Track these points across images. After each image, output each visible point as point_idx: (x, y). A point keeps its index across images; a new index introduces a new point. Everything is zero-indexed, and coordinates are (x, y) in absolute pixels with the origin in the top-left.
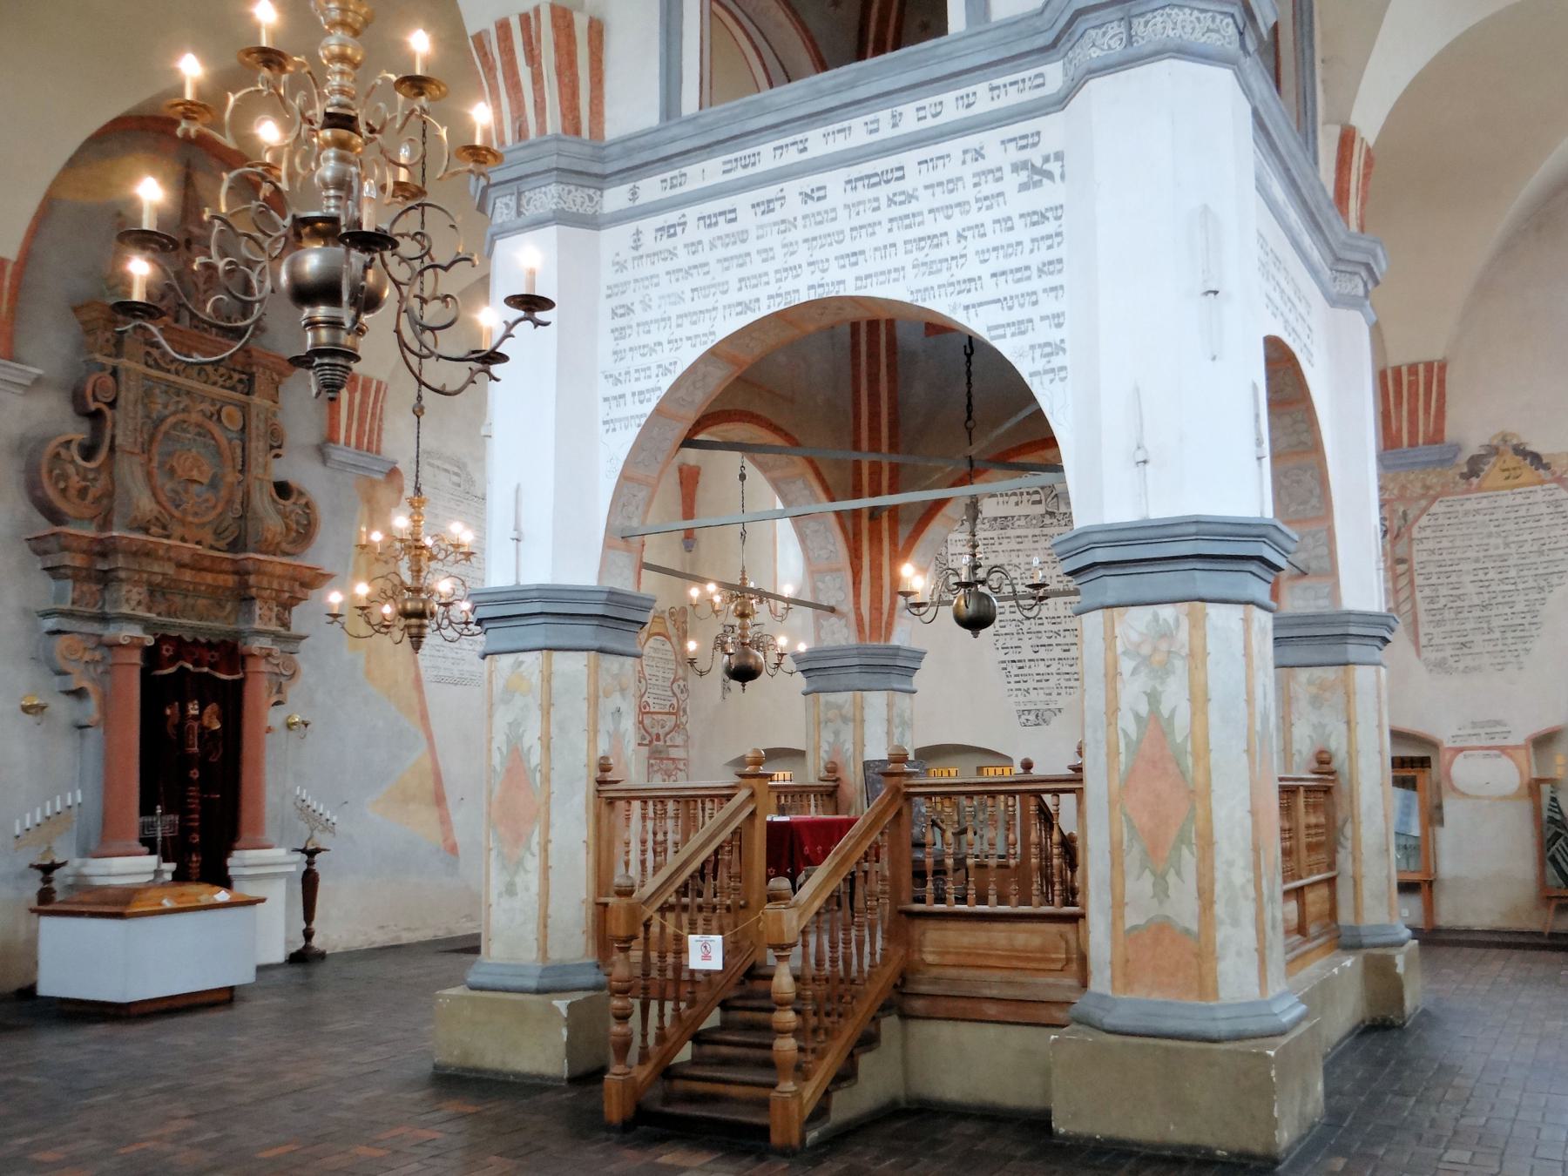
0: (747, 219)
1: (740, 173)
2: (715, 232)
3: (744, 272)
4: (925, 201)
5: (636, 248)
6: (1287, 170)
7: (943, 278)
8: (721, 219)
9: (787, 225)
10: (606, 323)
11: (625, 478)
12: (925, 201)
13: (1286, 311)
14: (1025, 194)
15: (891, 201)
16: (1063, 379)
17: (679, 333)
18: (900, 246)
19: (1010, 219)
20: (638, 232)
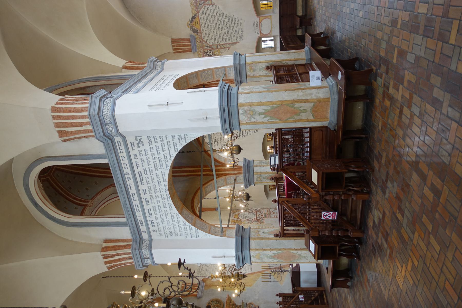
0: (150, 206)
1: (140, 208)
2: (153, 214)
3: (162, 207)
5: (157, 231)
6: (135, 83)
7: (164, 162)
8: (150, 212)
9: (151, 197)
10: (174, 238)
11: (209, 233)
12: (146, 167)
15: (146, 174)
17: (176, 221)
18: (156, 172)
20: (153, 231)
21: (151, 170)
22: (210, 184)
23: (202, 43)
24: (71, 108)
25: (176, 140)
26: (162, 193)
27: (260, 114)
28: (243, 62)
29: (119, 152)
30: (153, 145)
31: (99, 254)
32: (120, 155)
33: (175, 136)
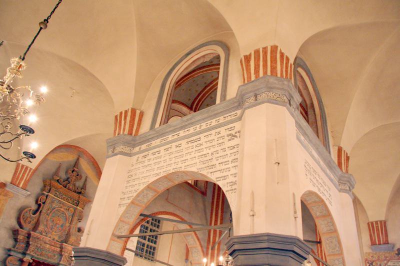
0: (163, 153)
2: (155, 156)
4: (205, 145)
7: (206, 165)
16: (235, 192)
19: (225, 148)
23: (385, 260)
24: (276, 63)
25: (231, 179)
26: (173, 164)
29: (225, 116)
30: (228, 152)
31: (129, 107)
32: (222, 118)
33: (235, 177)
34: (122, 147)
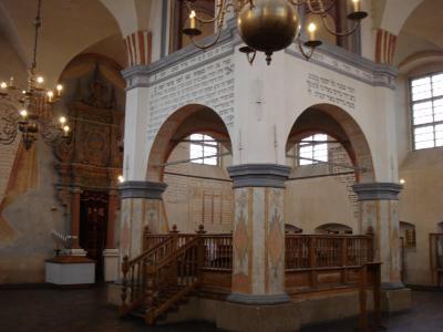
9: (182, 85)
10: (149, 112)
13: (326, 93)
14: (272, 62)
21: (204, 83)
22: (128, 157)
27: (242, 213)
28: (379, 196)
31: (135, 30)
34: (137, 78)
